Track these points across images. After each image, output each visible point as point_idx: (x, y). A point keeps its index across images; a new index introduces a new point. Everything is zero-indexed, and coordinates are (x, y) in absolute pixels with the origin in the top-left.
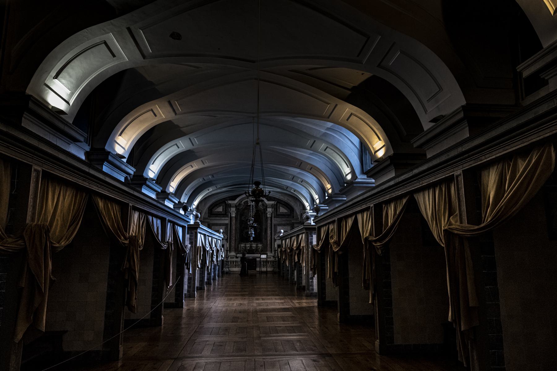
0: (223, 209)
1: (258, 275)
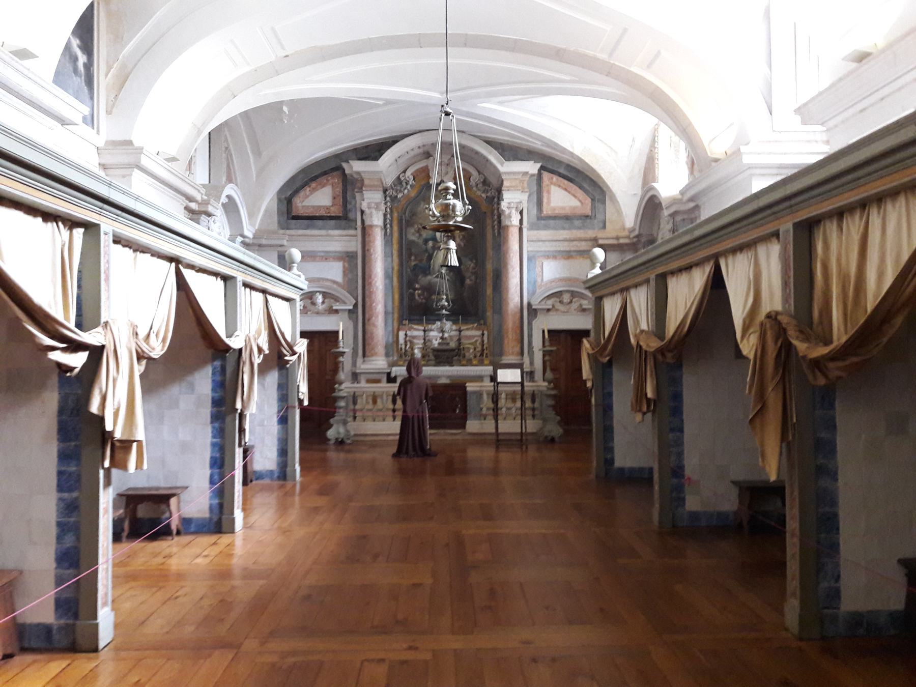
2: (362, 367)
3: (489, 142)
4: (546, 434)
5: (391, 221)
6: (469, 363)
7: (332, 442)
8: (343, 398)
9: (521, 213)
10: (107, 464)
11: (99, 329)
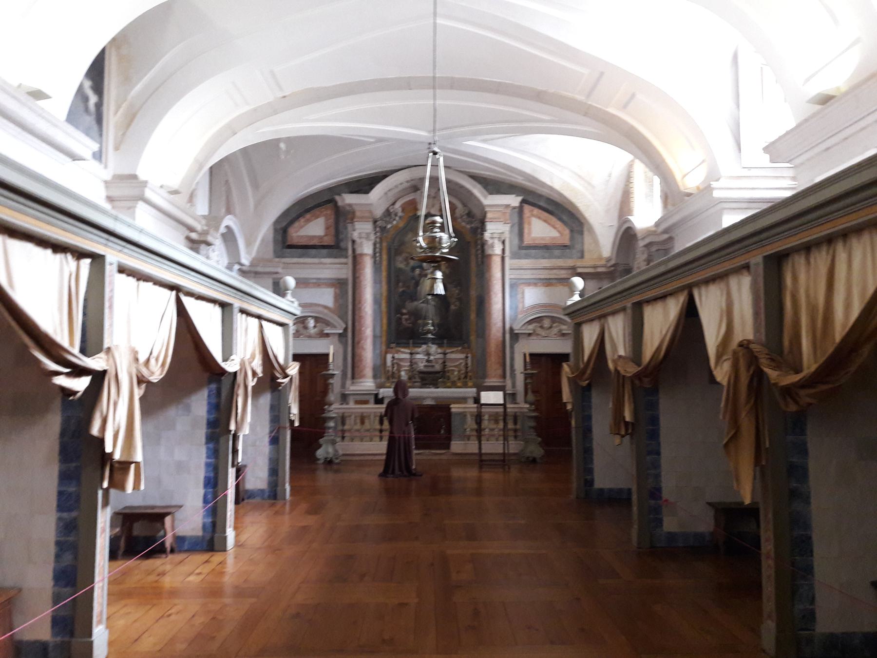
0: (327, 228)
2: (352, 388)
3: (475, 177)
4: (528, 455)
5: (381, 249)
6: (454, 385)
7: (322, 461)
8: (332, 418)
9: (503, 242)
10: (105, 485)
11: (102, 355)
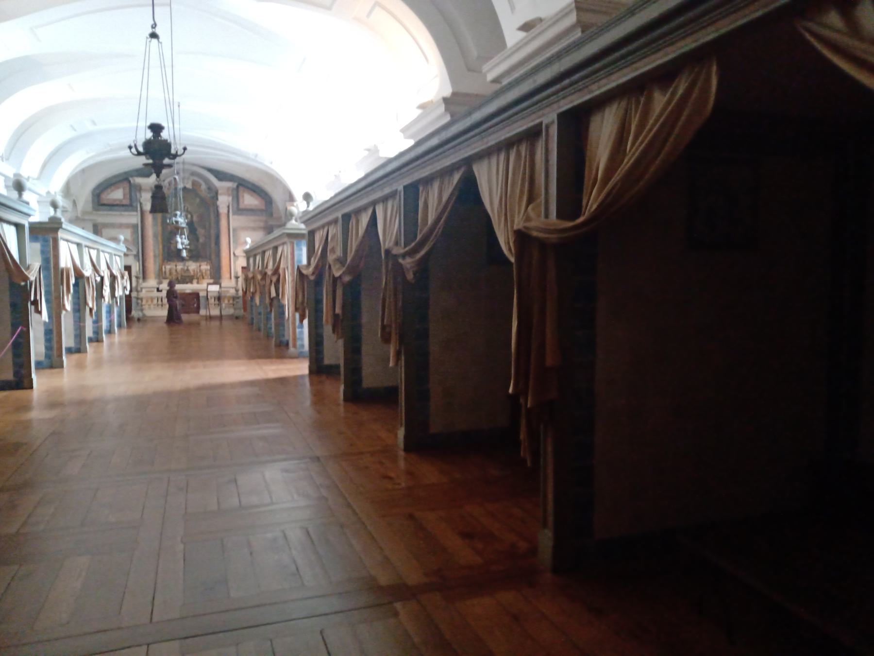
0: (124, 195)
1: (203, 323)
3: (210, 170)
